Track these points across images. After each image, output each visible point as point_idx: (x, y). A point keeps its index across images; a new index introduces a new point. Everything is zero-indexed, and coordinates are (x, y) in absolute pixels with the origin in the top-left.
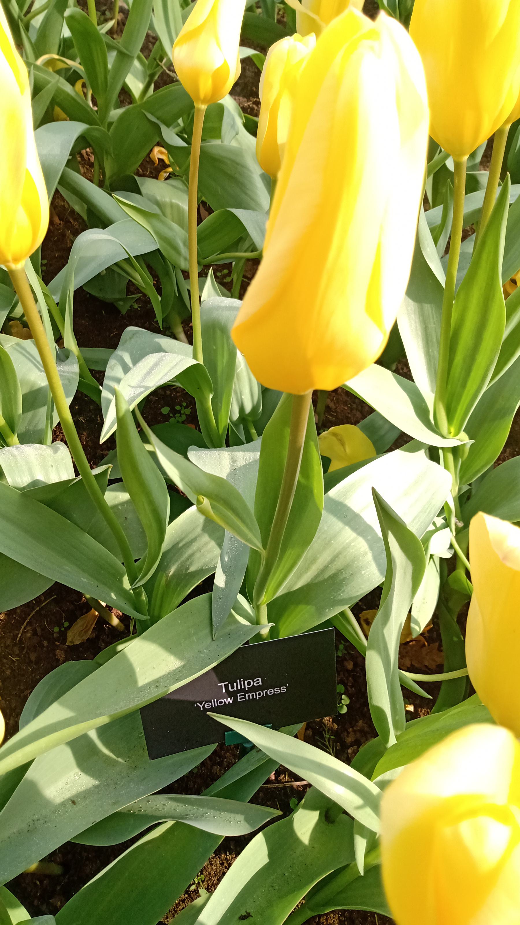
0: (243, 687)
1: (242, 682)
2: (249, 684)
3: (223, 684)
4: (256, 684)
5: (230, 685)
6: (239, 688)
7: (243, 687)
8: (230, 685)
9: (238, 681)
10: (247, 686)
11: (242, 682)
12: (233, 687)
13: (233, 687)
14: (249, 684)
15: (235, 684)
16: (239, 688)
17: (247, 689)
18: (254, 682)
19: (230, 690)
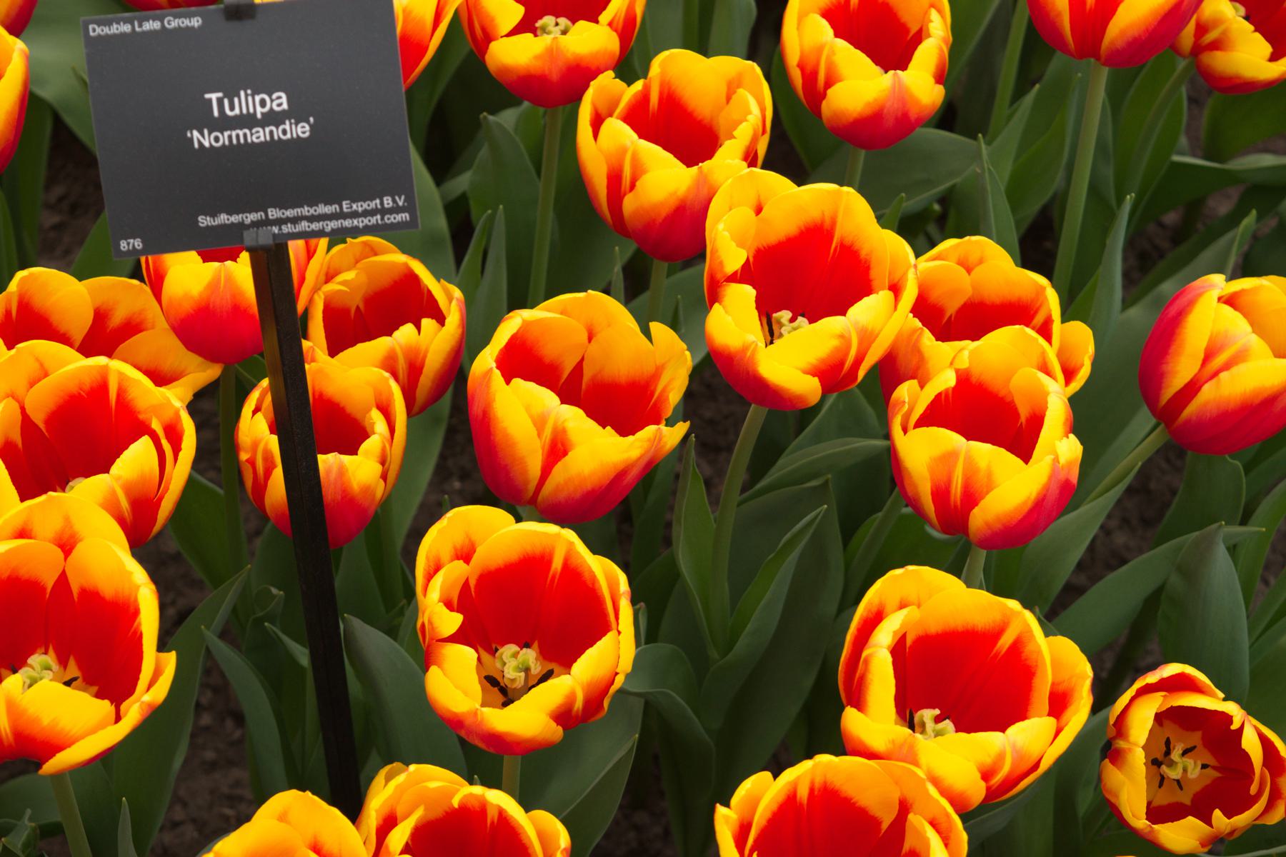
0: (251, 110)
1: (250, 99)
2: (263, 103)
3: (214, 96)
4: (279, 105)
5: (226, 102)
6: (245, 111)
7: (251, 110)
8: (226, 102)
9: (242, 93)
10: (259, 110)
11: (250, 99)
12: (232, 108)
13: (232, 108)
14: (263, 103)
15: (236, 100)
16: (245, 111)
17: (259, 116)
18: (272, 101)
19: (228, 112)
